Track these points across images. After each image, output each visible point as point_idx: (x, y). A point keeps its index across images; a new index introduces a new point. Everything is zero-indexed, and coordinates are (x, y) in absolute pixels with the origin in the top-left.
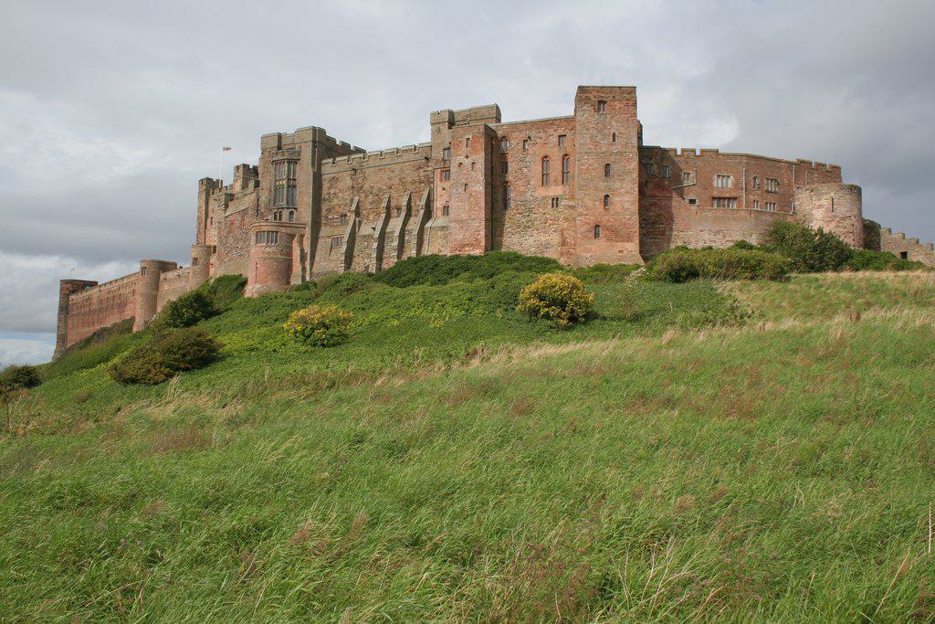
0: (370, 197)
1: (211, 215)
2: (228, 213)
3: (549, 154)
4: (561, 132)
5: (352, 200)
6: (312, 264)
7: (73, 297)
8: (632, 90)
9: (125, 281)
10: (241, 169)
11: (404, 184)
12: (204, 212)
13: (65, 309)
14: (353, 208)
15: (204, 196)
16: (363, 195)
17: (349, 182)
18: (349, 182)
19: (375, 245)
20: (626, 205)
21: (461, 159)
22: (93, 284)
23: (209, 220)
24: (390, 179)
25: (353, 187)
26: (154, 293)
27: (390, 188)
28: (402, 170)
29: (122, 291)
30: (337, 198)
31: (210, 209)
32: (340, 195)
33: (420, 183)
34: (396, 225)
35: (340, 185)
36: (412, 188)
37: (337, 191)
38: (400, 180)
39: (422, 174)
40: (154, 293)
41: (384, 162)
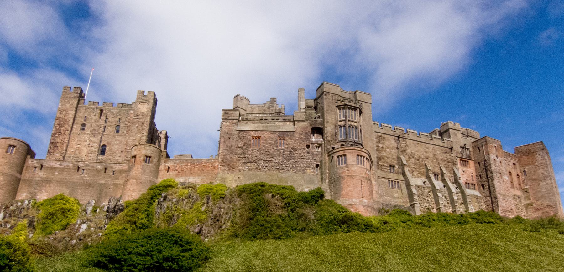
0: (413, 159)
1: (80, 120)
11: (437, 159)
12: (71, 116)
15: (74, 102)
18: (394, 144)
23: (77, 127)
24: (426, 152)
25: (397, 148)
26: (18, 176)
27: (427, 158)
28: (434, 150)
30: (385, 151)
31: (79, 114)
32: (388, 150)
33: (449, 162)
35: (387, 143)
37: (384, 146)
38: (434, 155)
39: (449, 157)
40: (18, 176)
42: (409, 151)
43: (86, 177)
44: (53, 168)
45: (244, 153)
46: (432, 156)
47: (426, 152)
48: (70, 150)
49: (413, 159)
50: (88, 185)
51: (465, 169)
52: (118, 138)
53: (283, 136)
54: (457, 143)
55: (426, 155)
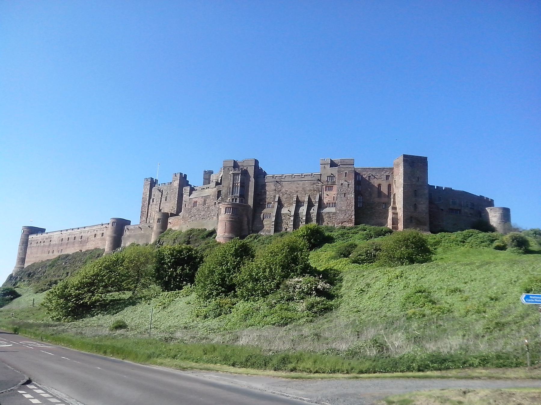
0: (285, 195)
1: (153, 197)
2: (191, 197)
3: (381, 183)
4: (387, 174)
5: (275, 196)
6: (252, 225)
7: (30, 237)
8: (426, 159)
9: (87, 229)
10: (178, 176)
12: (148, 195)
13: (25, 244)
14: (277, 200)
16: (281, 194)
17: (273, 187)
18: (273, 187)
19: (292, 218)
20: (424, 209)
21: (343, 182)
22: (42, 231)
24: (297, 188)
28: (304, 184)
29: (82, 234)
34: (303, 210)
36: (310, 193)
38: (303, 188)
41: (293, 180)
42: (283, 190)
43: (142, 232)
44: (132, 229)
45: (190, 212)
46: (301, 189)
47: (297, 188)
48: (149, 214)
49: (285, 195)
50: (142, 236)
51: (328, 193)
52: (167, 204)
53: (206, 198)
54: (324, 174)
55: (296, 190)
